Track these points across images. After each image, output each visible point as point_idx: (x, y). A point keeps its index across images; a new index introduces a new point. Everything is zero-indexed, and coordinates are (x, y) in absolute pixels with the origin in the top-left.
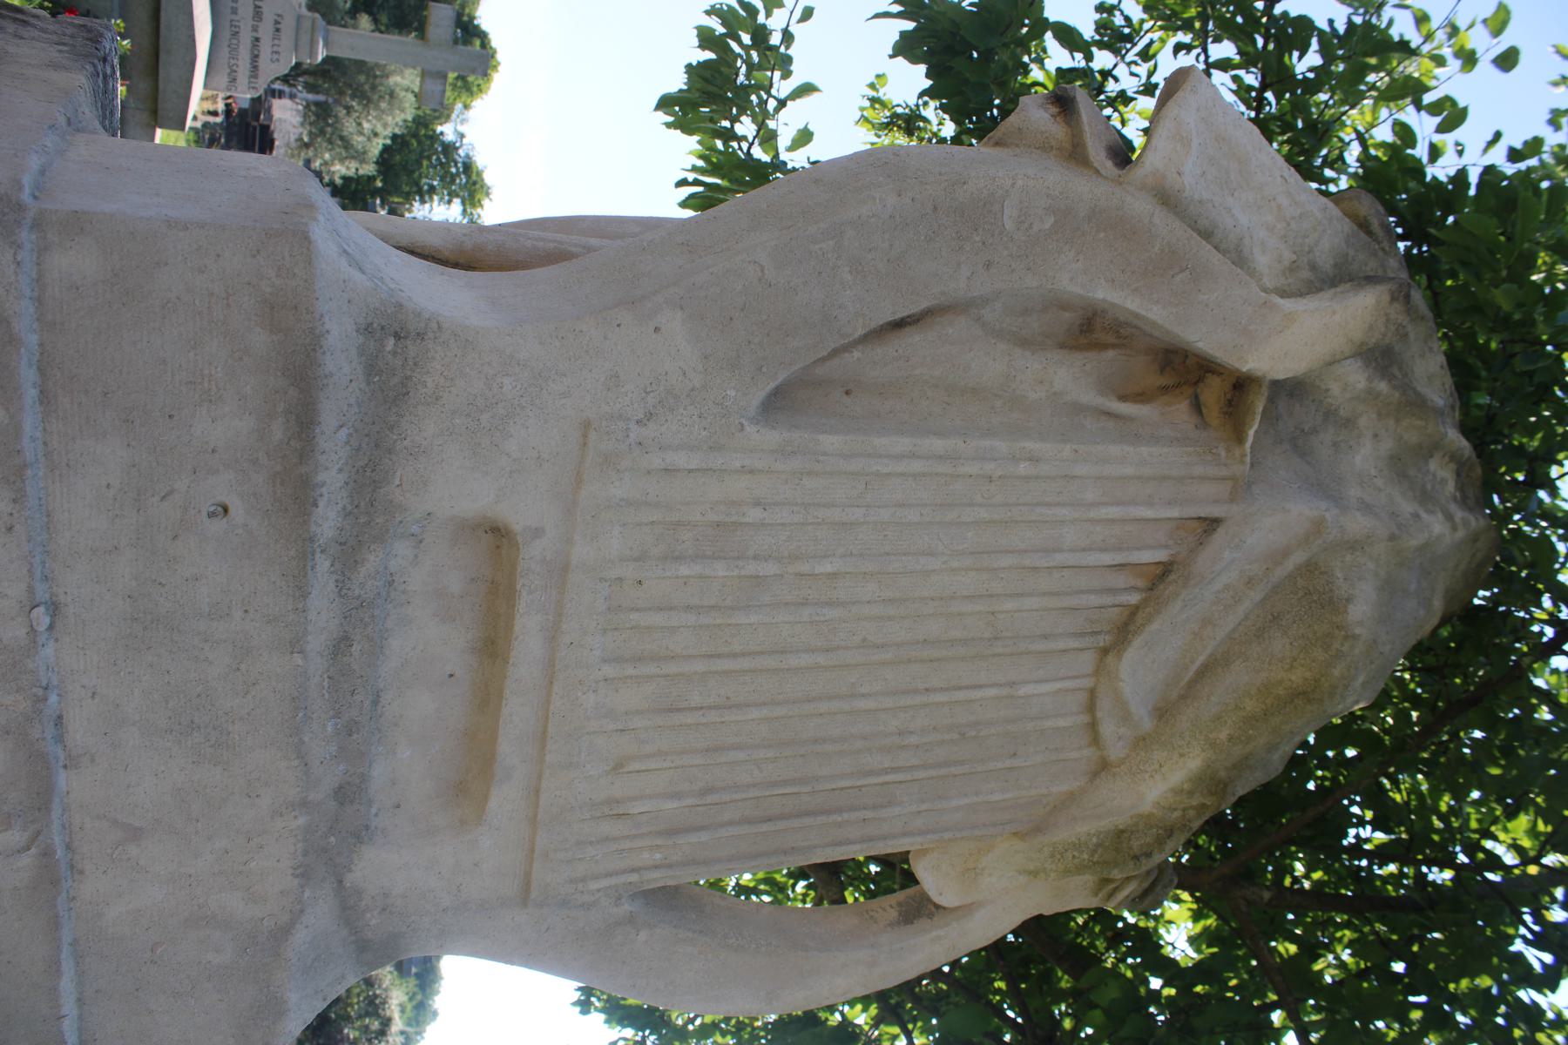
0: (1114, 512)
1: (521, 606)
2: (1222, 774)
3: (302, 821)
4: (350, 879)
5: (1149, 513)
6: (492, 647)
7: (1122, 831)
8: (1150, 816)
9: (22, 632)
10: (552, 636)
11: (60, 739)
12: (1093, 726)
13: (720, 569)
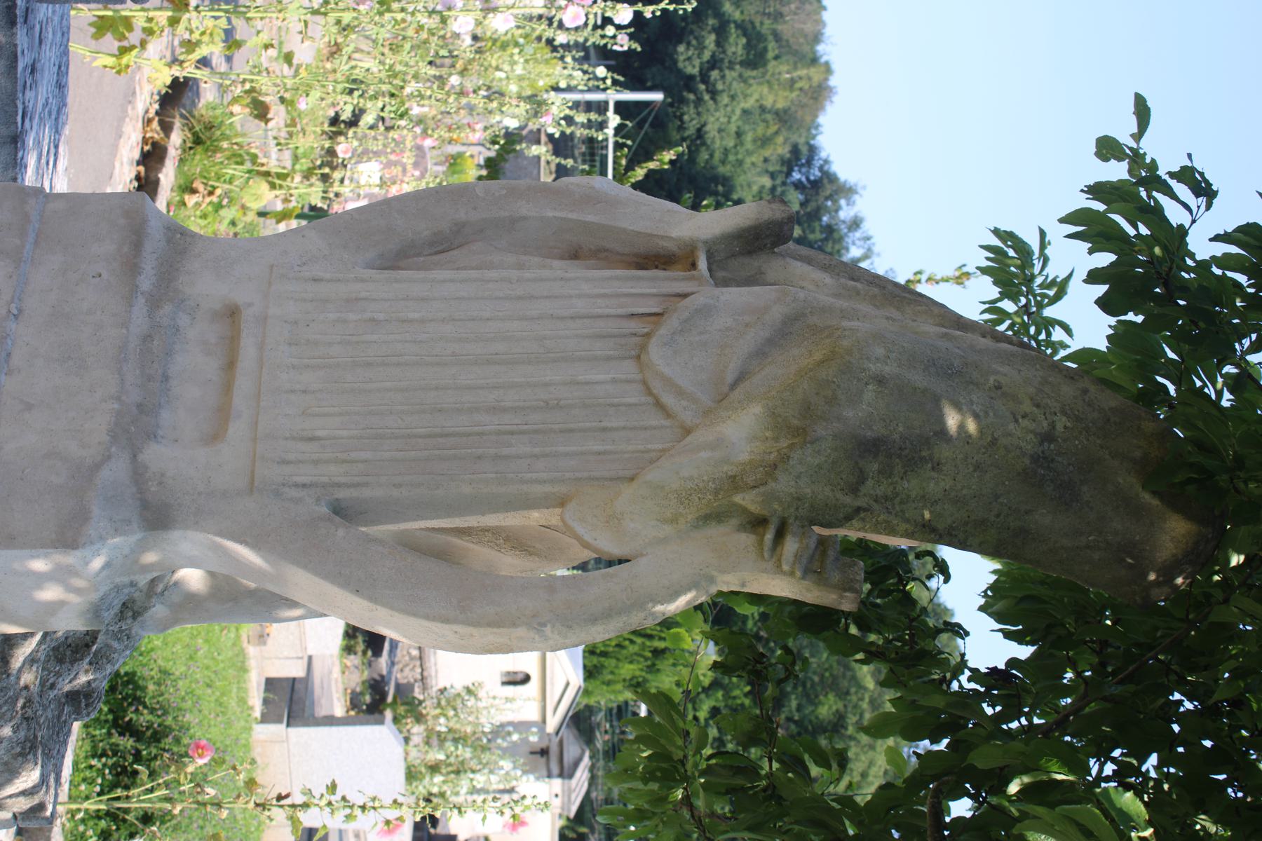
0: (602, 291)
1: (244, 335)
2: (796, 422)
3: (116, 406)
4: (141, 457)
5: (633, 291)
6: (230, 365)
7: (734, 477)
8: (751, 462)
9: (4, 312)
10: (261, 347)
11: (7, 361)
12: (658, 404)
13: (351, 316)
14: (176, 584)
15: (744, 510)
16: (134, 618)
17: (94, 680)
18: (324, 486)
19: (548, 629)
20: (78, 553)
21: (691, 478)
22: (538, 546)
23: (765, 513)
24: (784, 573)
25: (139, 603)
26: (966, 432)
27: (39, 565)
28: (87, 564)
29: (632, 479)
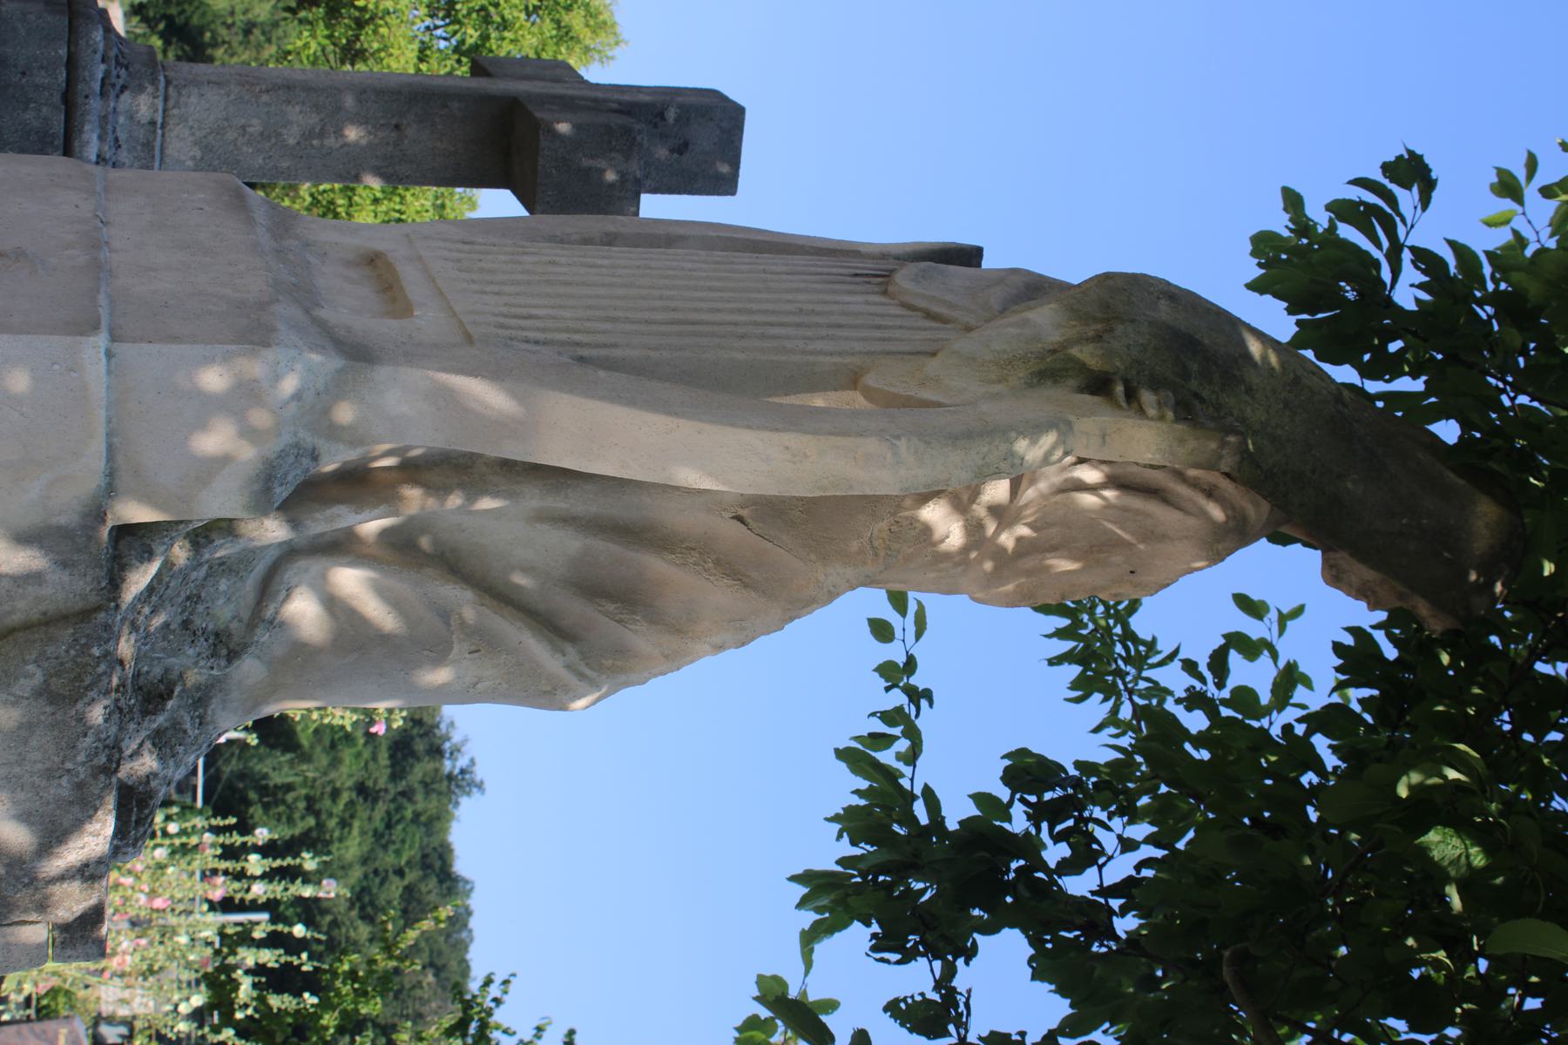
2: (1099, 315)
14: (282, 624)
15: (1082, 367)
16: (230, 660)
17: (155, 775)
18: (562, 343)
19: (902, 444)
20: (269, 354)
21: (1004, 351)
22: (754, 574)
23: (1107, 368)
24: (1152, 419)
25: (236, 639)
26: (1269, 363)
27: (214, 379)
28: (277, 378)
29: (933, 354)
